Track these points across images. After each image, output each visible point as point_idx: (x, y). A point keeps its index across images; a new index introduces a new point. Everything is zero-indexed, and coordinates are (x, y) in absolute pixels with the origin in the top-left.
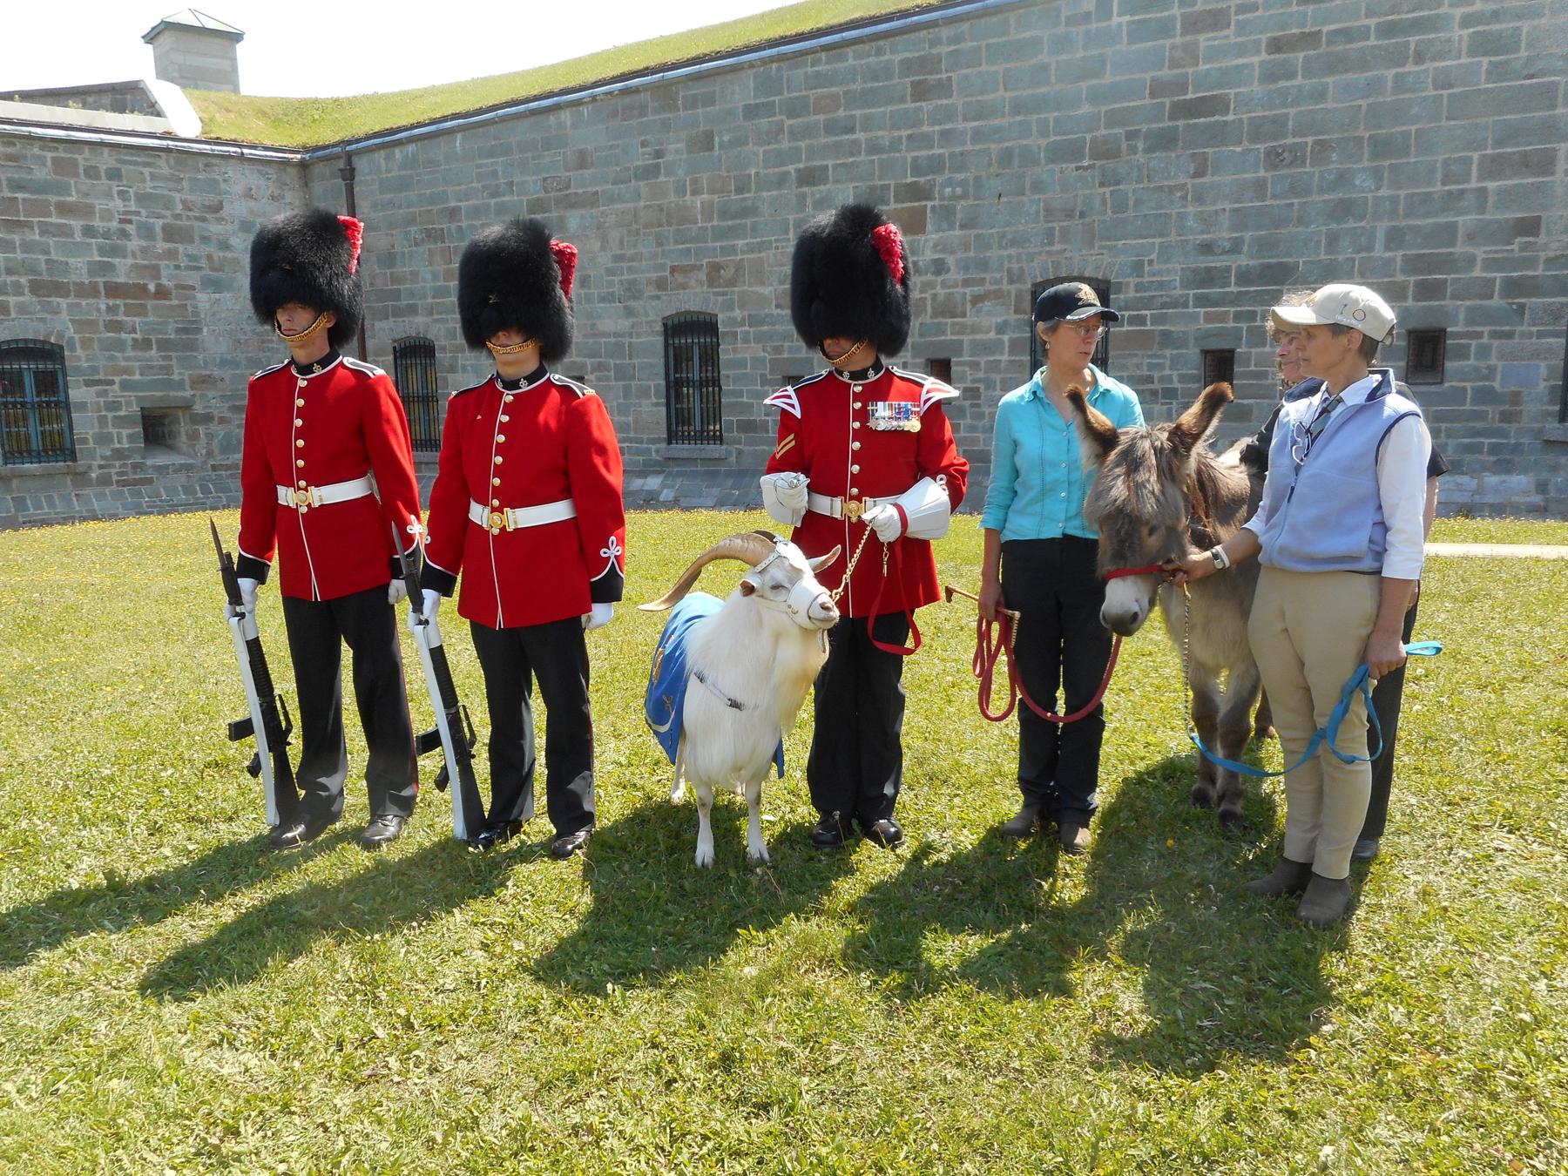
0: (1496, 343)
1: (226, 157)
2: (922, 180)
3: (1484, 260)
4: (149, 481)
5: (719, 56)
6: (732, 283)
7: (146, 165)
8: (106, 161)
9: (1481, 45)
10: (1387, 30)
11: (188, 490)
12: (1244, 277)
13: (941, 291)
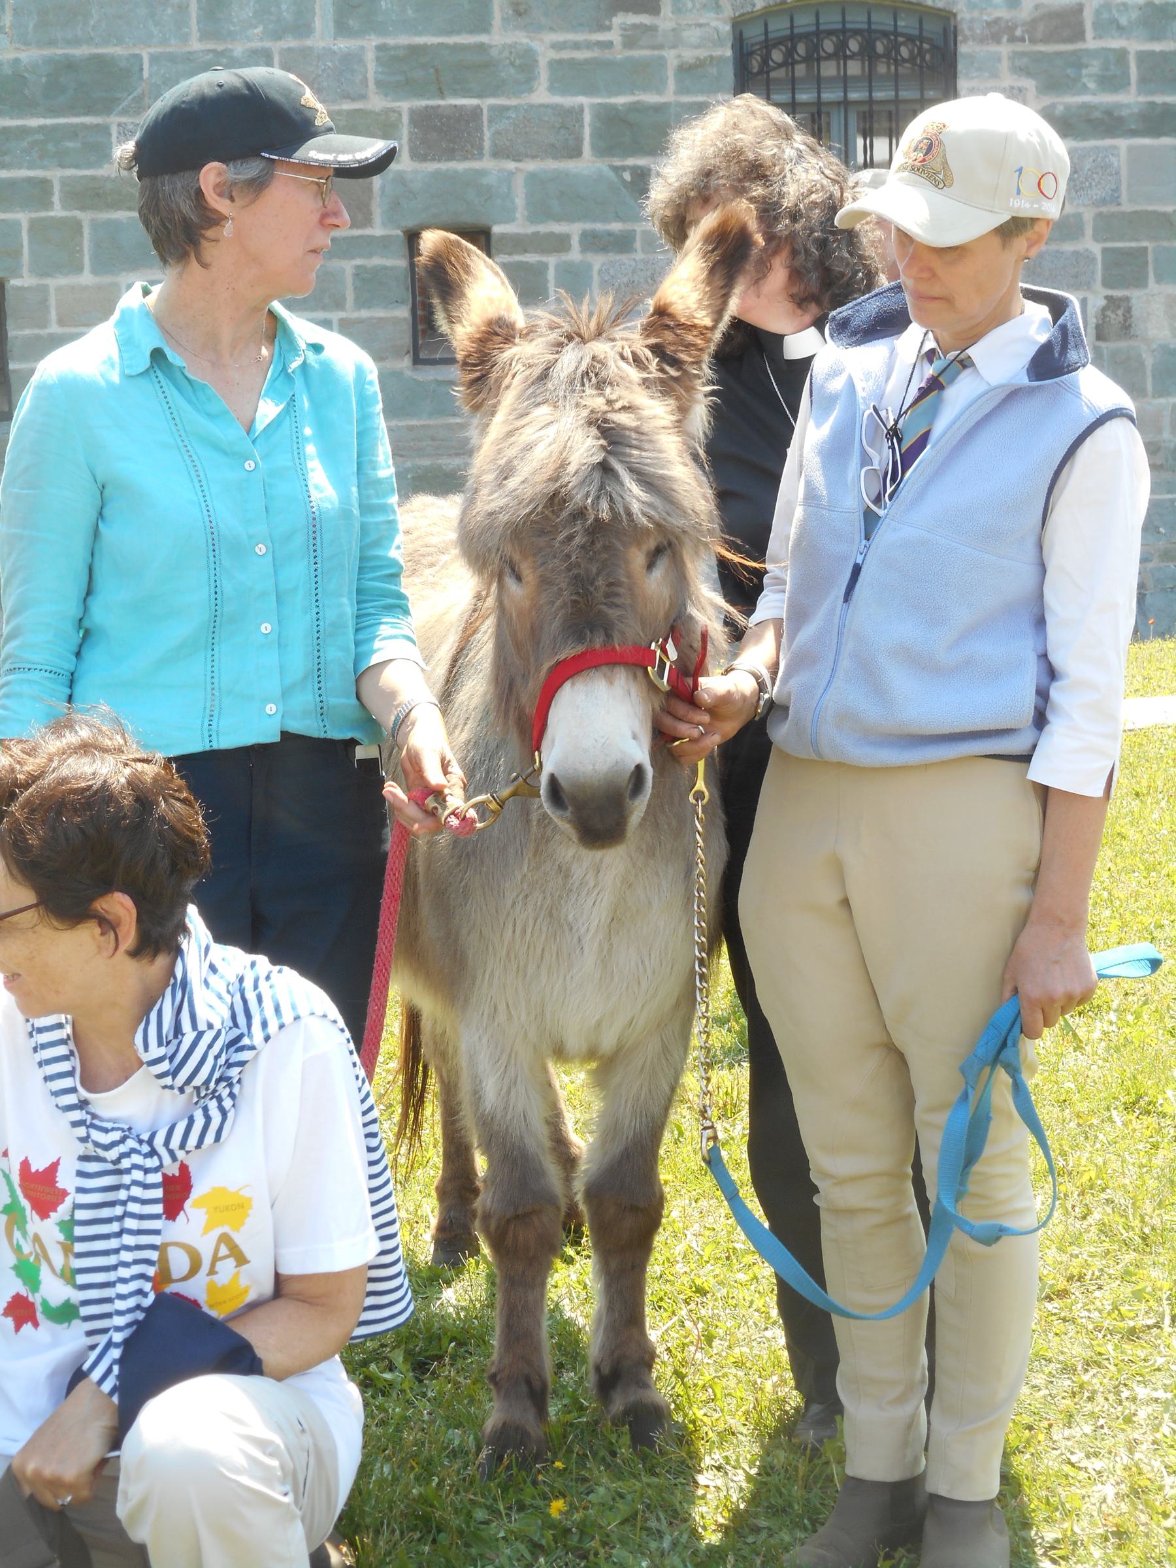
0: (597, 261)
3: (555, 65)
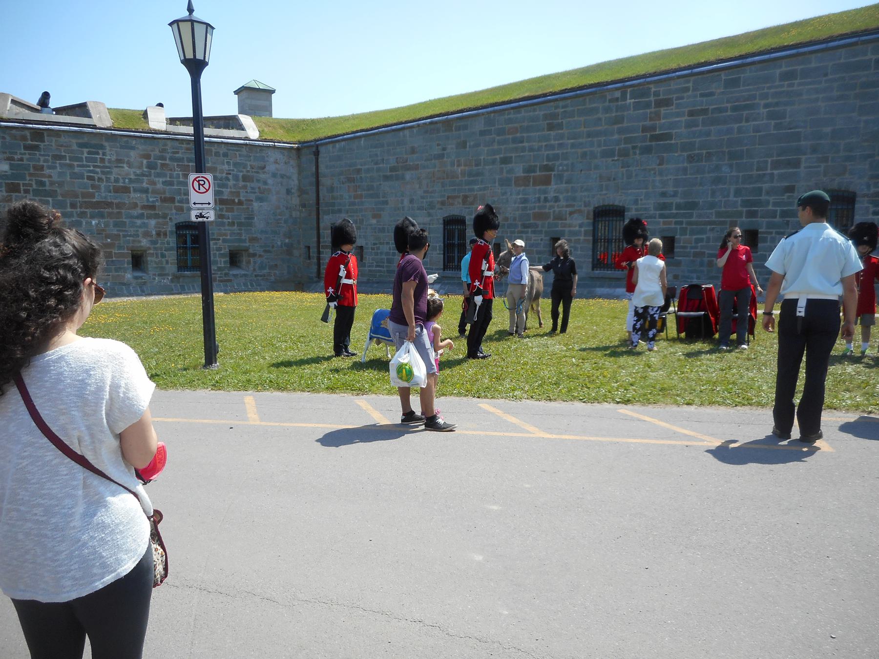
1: (269, 147)
2: (550, 163)
4: (230, 281)
5: (470, 110)
6: (472, 203)
7: (237, 151)
8: (223, 150)
9: (771, 116)
10: (735, 109)
11: (245, 285)
12: (679, 207)
13: (557, 209)
